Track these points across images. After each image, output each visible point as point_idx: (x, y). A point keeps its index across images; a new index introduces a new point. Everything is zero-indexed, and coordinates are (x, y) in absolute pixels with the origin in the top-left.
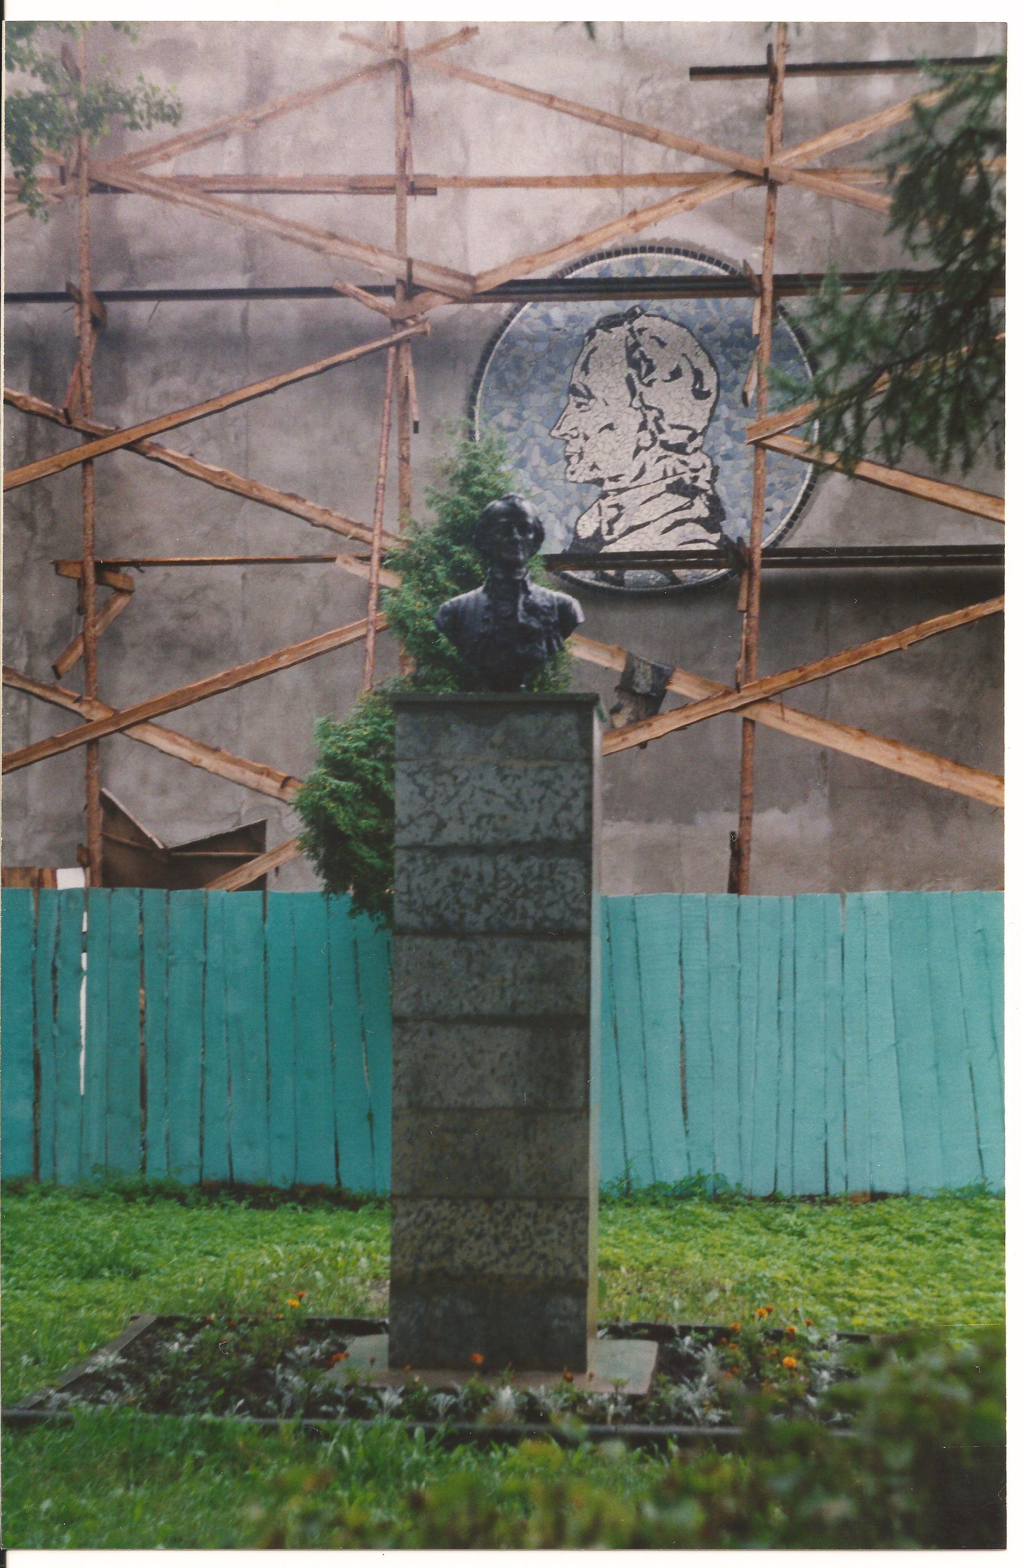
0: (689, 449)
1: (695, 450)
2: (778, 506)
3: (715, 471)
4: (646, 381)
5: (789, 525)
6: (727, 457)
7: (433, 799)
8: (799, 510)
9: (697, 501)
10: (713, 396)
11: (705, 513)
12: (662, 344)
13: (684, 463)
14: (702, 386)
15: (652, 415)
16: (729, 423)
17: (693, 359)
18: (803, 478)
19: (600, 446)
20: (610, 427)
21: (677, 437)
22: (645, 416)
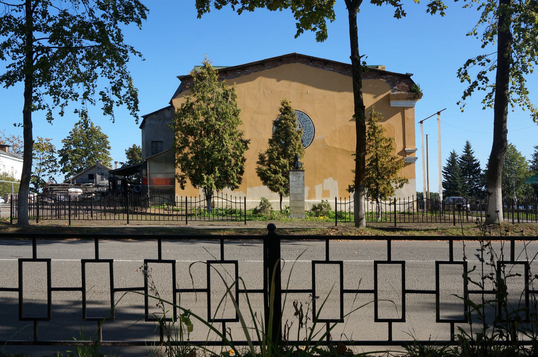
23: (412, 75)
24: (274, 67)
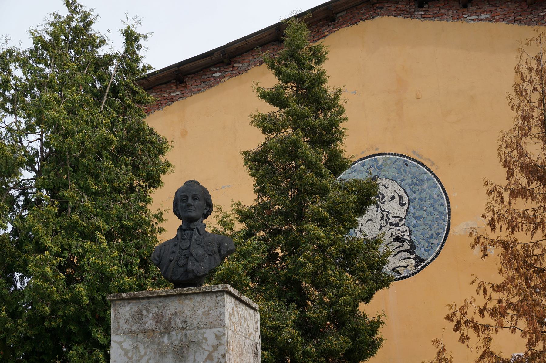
0: (400, 225)
1: (402, 225)
2: (436, 242)
3: (410, 231)
4: (382, 202)
5: (441, 249)
6: (415, 226)
7: (132, 357)
8: (444, 243)
9: (405, 243)
10: (407, 204)
11: (409, 248)
12: (387, 188)
13: (399, 230)
14: (402, 201)
15: (385, 214)
16: (414, 214)
17: (399, 192)
18: (444, 230)
19: (367, 227)
20: (370, 220)
21: (393, 221)
22: (383, 214)
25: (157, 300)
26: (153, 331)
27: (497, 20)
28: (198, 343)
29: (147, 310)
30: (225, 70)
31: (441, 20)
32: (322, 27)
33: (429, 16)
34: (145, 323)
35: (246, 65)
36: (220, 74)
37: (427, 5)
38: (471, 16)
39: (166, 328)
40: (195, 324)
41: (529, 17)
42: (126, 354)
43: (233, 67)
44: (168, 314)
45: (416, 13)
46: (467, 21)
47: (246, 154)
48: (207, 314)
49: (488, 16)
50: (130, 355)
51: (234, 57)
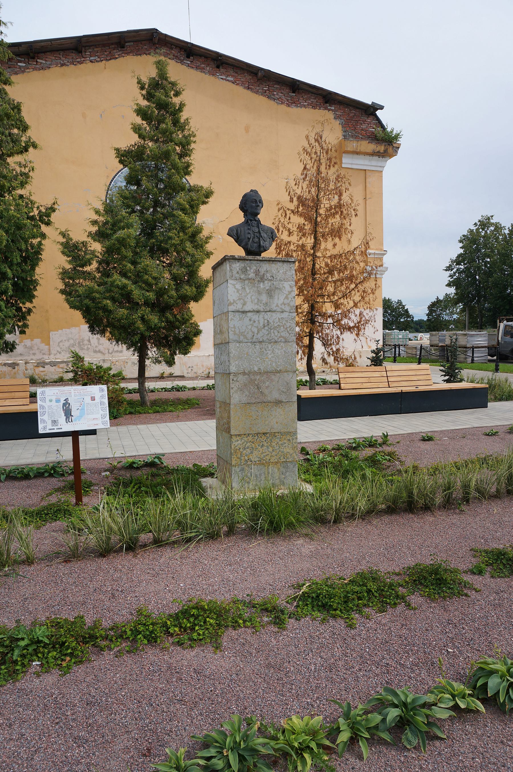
7: (242, 294)
23: (382, 108)
24: (107, 60)
25: (256, 262)
26: (254, 280)
27: (238, 84)
28: (280, 289)
29: (249, 267)
30: (30, 63)
31: (201, 72)
32: (114, 50)
33: (193, 66)
34: (249, 275)
35: (48, 63)
36: (24, 65)
37: (192, 58)
38: (221, 75)
39: (261, 279)
40: (278, 279)
41: (258, 88)
42: (238, 291)
43: (37, 62)
44: (262, 271)
45: (185, 61)
46: (219, 78)
47: (117, 150)
48: (285, 273)
49: (232, 79)
50: (240, 292)
51: (38, 53)
